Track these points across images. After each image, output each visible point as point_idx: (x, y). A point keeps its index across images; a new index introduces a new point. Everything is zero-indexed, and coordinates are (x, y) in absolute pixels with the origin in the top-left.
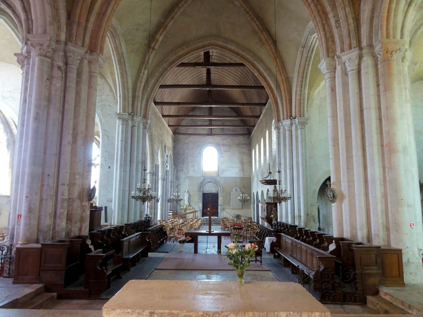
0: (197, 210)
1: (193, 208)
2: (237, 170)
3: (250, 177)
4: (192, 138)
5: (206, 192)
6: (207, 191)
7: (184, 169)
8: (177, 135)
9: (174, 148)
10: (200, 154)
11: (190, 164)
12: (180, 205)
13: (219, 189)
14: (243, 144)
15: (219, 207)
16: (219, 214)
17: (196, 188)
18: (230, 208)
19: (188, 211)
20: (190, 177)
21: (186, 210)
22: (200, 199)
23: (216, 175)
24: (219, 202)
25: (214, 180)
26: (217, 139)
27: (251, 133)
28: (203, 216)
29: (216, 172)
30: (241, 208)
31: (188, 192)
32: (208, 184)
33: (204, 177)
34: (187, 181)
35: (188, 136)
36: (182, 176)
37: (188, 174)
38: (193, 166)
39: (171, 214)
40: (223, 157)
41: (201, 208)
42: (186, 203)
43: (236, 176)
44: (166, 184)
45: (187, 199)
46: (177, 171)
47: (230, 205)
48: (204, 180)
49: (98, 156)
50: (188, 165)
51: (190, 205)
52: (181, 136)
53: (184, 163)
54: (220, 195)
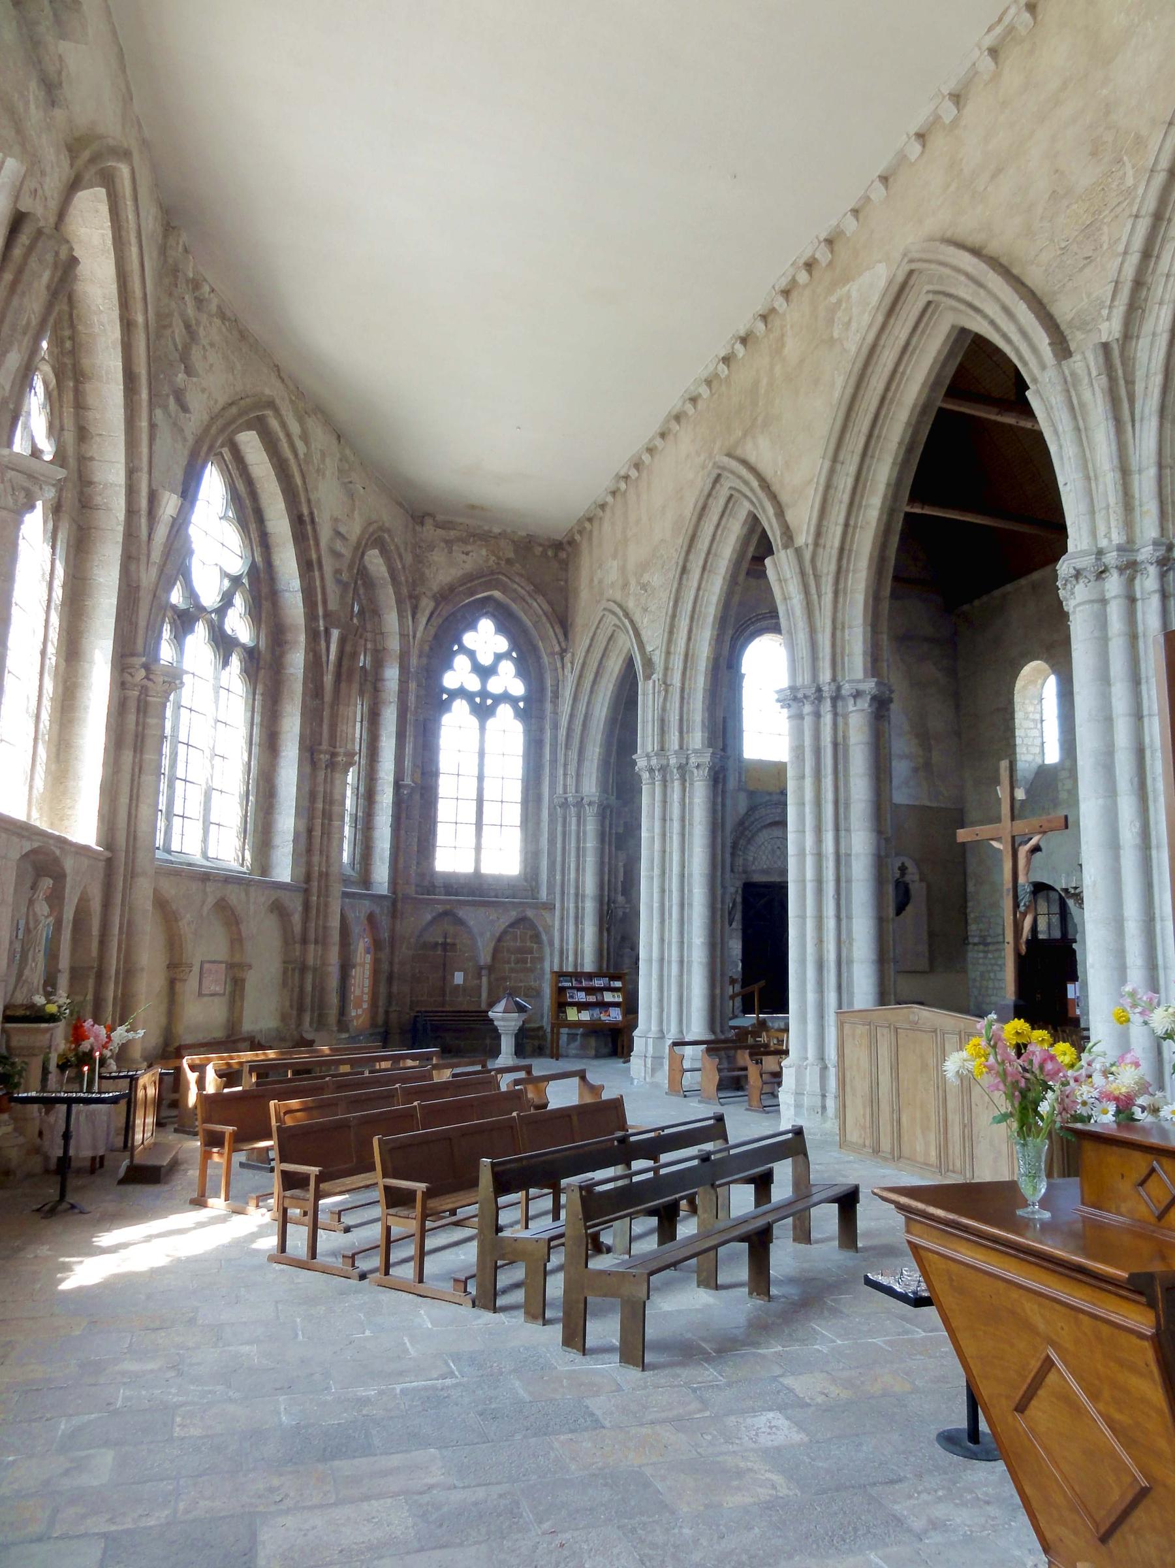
5: (758, 878)
33: (751, 794)
39: (618, 998)
48: (752, 809)
49: (236, 581)
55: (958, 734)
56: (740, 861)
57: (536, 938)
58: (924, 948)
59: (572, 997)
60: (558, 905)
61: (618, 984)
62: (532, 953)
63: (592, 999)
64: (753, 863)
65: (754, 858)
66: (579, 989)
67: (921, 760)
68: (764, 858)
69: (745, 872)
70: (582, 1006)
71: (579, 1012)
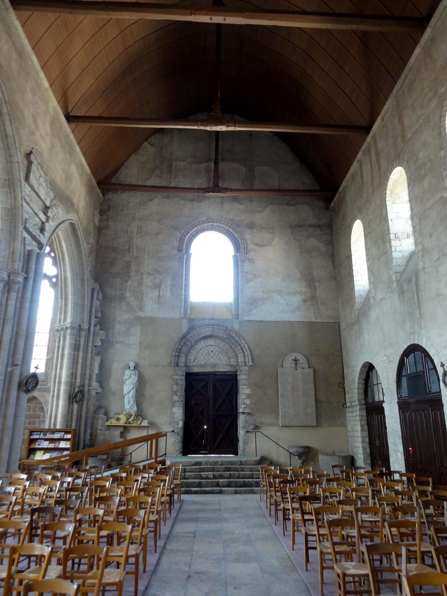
0: (165, 429)
1: (152, 425)
2: (296, 300)
3: (339, 324)
4: (157, 205)
5: (196, 370)
6: (202, 366)
7: (128, 295)
8: (110, 196)
9: (100, 231)
10: (183, 251)
11: (147, 281)
12: (106, 414)
13: (241, 359)
14: (310, 226)
15: (241, 419)
16: (241, 444)
17: (163, 355)
18: (277, 425)
19: (133, 435)
20: (145, 318)
21: (126, 428)
22: (175, 393)
23: (230, 317)
24: (240, 401)
25: (221, 329)
26: (234, 210)
27: (337, 189)
28: (185, 452)
29: (227, 307)
30: (315, 424)
31: (135, 368)
32: (202, 343)
33: (191, 320)
34: (137, 331)
35: (146, 195)
36: (121, 315)
37: (141, 309)
38: (158, 287)
39: (67, 445)
40: (251, 261)
41: (181, 424)
42: (129, 405)
43: (296, 317)
44: (21, 308)
45: (132, 393)
46: (106, 299)
47: (274, 411)
48: (191, 328)
50: (140, 284)
51: (140, 414)
52: (124, 197)
53: (126, 276)
54: (242, 378)
55: (335, 278)
56: (182, 360)
57: (42, 409)
58: (312, 410)
59: (39, 445)
60: (52, 389)
61: (69, 436)
62: (39, 418)
63: (52, 446)
64: (194, 361)
65: (195, 358)
66: (46, 440)
67: (309, 295)
68: (202, 357)
69: (186, 366)
70: (46, 450)
71: (44, 454)
